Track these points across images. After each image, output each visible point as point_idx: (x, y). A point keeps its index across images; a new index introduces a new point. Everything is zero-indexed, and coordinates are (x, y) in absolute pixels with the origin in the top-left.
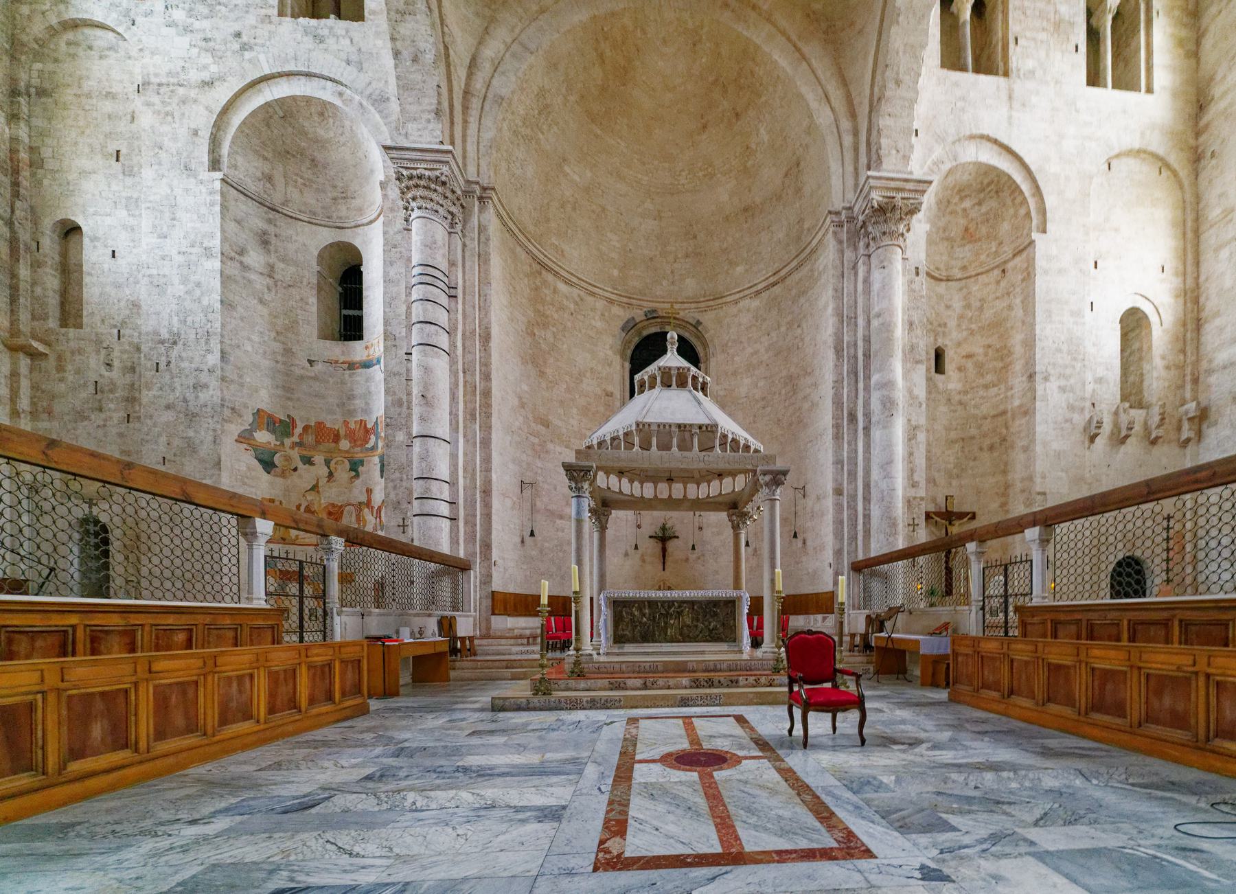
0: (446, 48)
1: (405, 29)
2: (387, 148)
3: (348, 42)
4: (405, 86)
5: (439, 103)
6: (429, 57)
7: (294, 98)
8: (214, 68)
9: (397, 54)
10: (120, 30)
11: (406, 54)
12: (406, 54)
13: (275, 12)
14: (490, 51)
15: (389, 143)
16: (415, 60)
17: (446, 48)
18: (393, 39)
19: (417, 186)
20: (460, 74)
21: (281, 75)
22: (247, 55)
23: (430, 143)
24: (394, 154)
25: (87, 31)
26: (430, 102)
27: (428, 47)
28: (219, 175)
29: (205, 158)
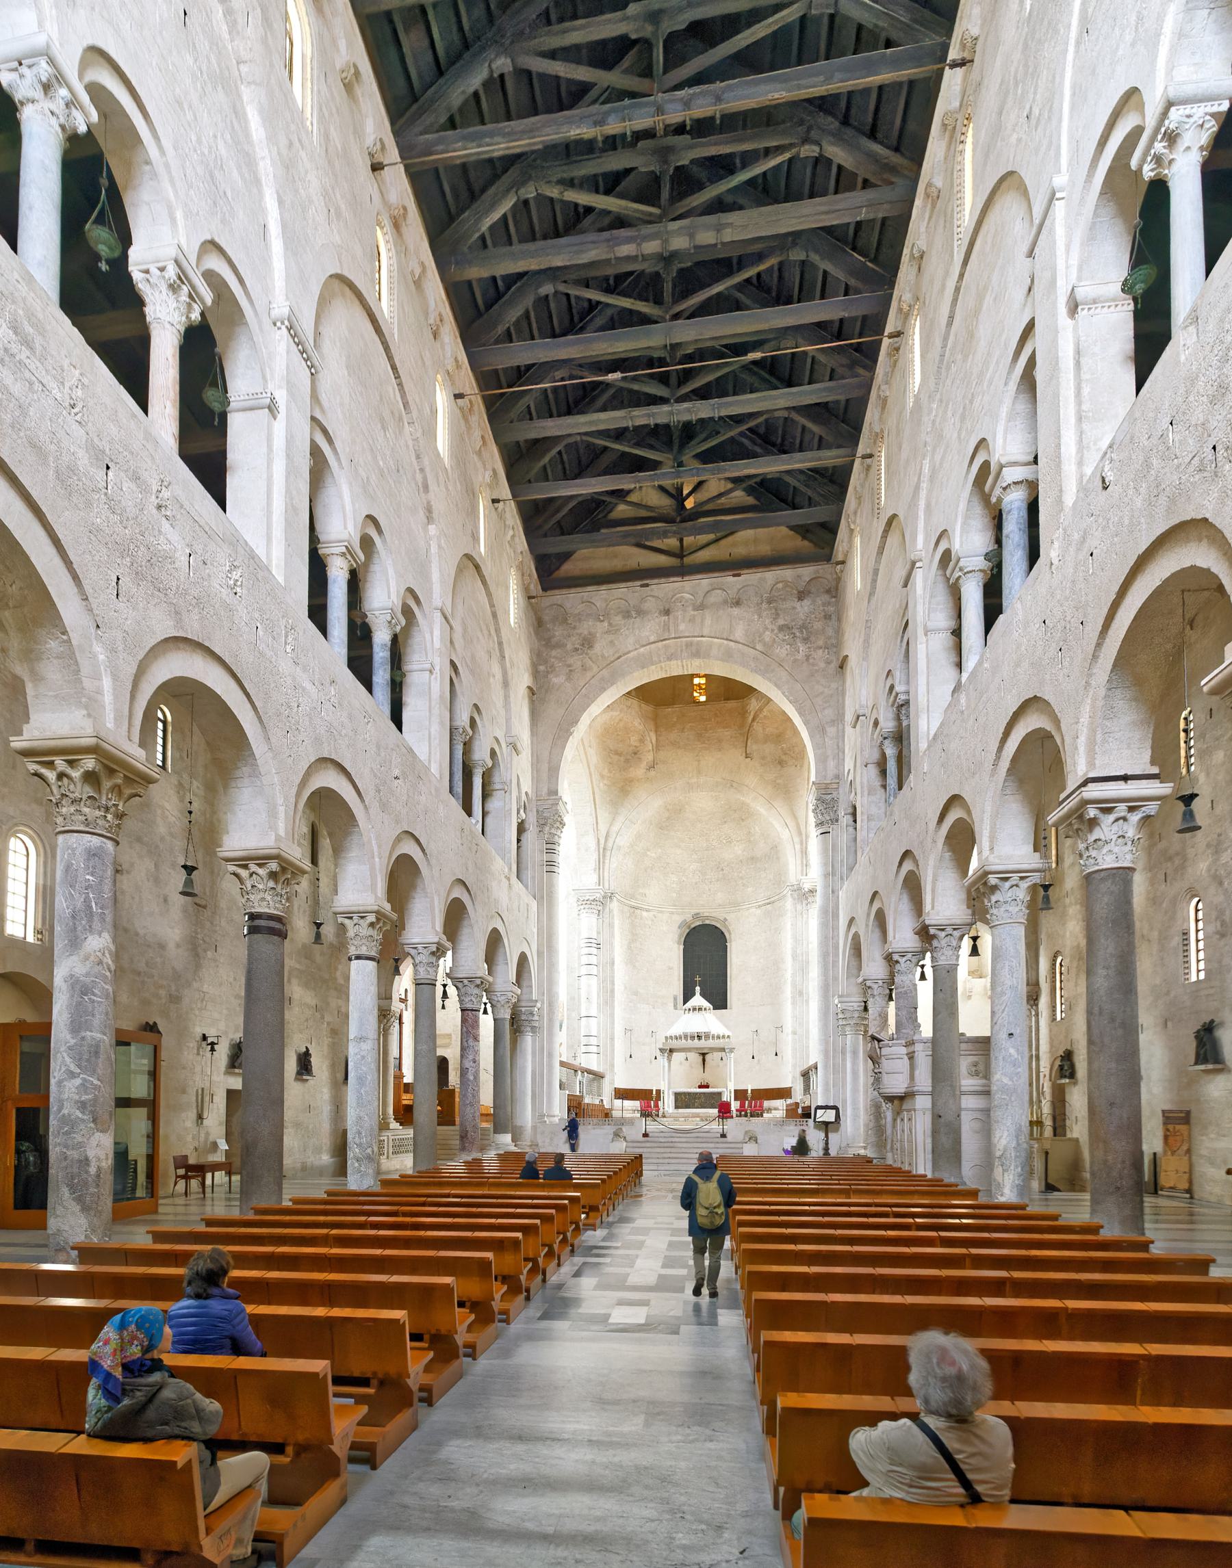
14: (615, 828)
20: (602, 842)
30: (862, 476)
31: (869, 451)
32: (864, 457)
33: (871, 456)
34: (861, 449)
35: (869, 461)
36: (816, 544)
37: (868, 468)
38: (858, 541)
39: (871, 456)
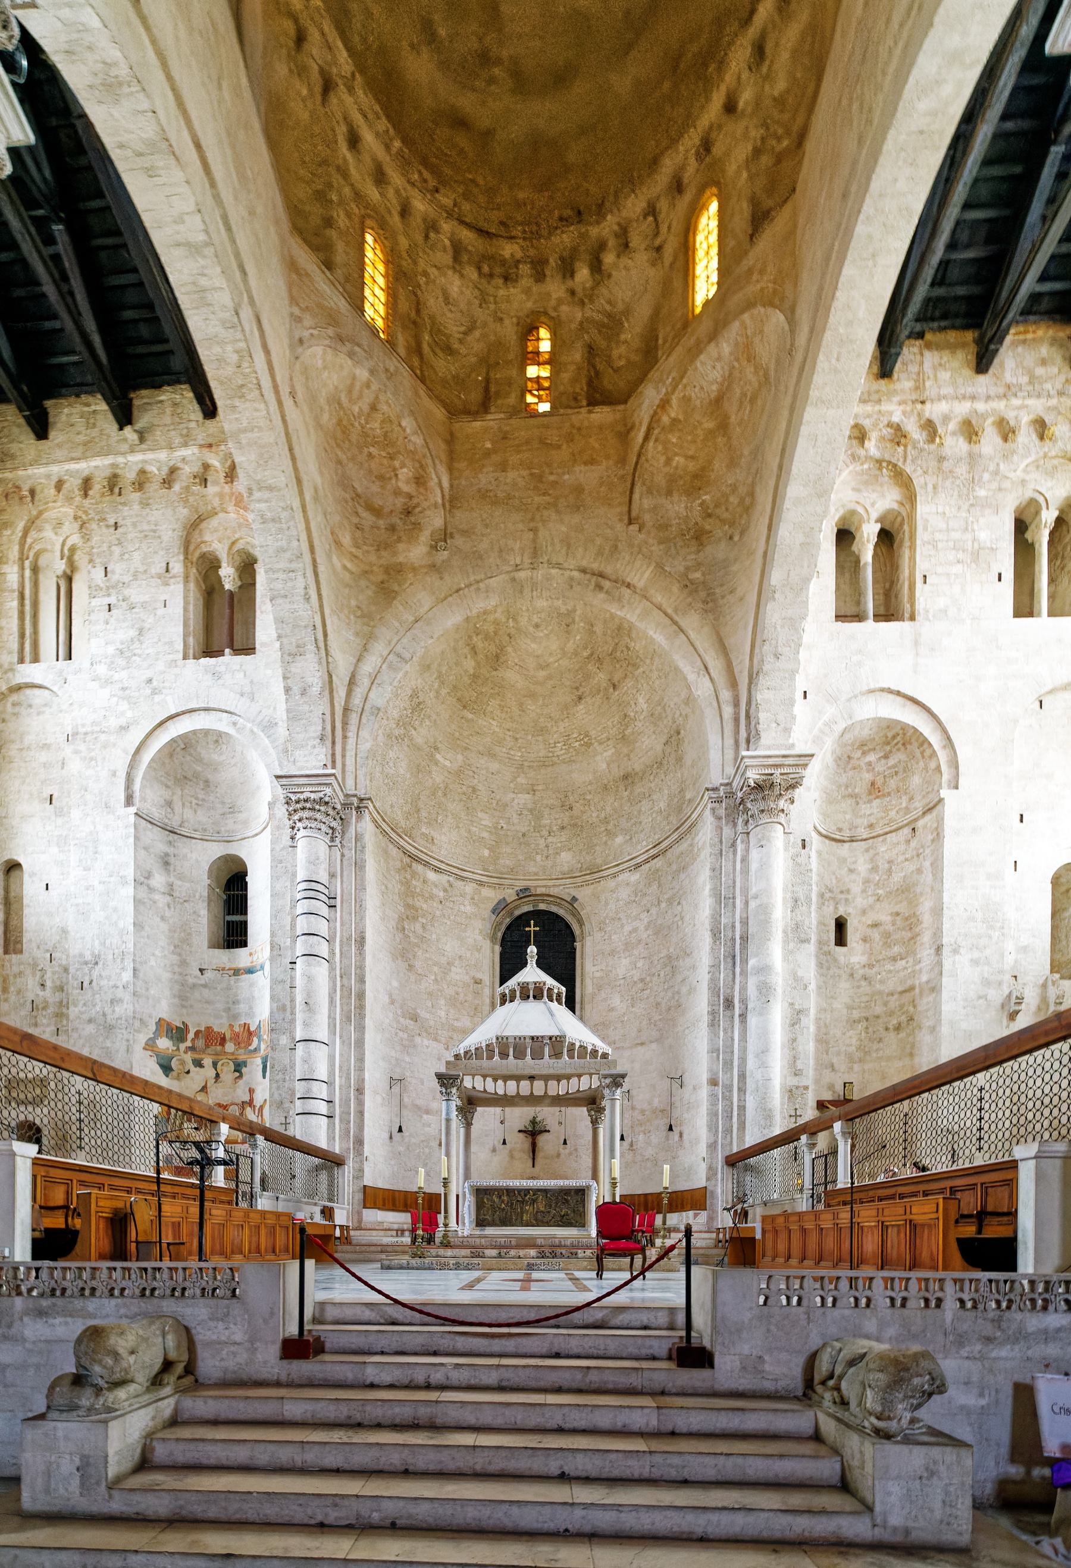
0: (330, 676)
1: (296, 668)
2: (278, 777)
3: (242, 675)
4: (293, 716)
5: (324, 729)
6: (316, 690)
7: (194, 732)
8: (129, 714)
9: (287, 690)
10: (55, 689)
11: (296, 690)
12: (296, 690)
13: (181, 656)
14: (368, 666)
15: (280, 773)
16: (304, 692)
17: (330, 676)
18: (285, 678)
19: (304, 809)
20: (341, 693)
21: (184, 713)
22: (157, 698)
23: (315, 767)
24: (284, 781)
25: (28, 691)
26: (316, 729)
27: (316, 680)
28: (132, 810)
29: (122, 797)
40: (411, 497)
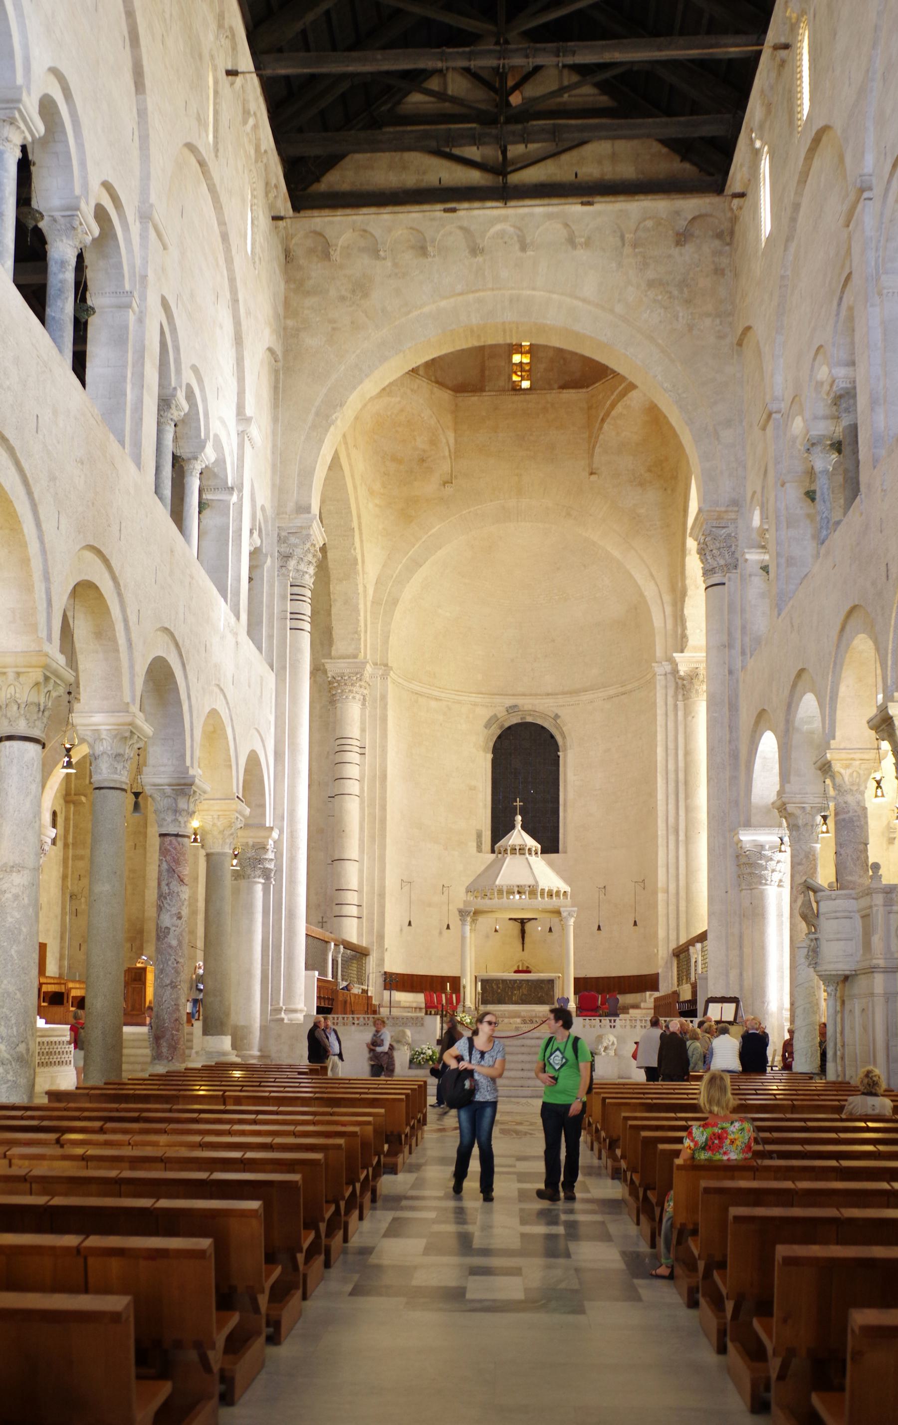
30: (773, 75)
31: (783, 40)
32: (777, 47)
33: (786, 47)
34: (773, 36)
35: (783, 53)
36: (701, 170)
37: (783, 63)
38: (765, 166)
39: (786, 47)
40: (424, 451)
